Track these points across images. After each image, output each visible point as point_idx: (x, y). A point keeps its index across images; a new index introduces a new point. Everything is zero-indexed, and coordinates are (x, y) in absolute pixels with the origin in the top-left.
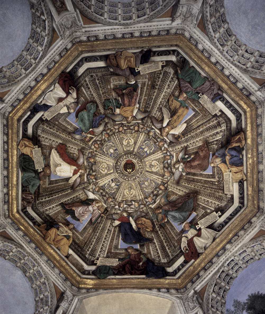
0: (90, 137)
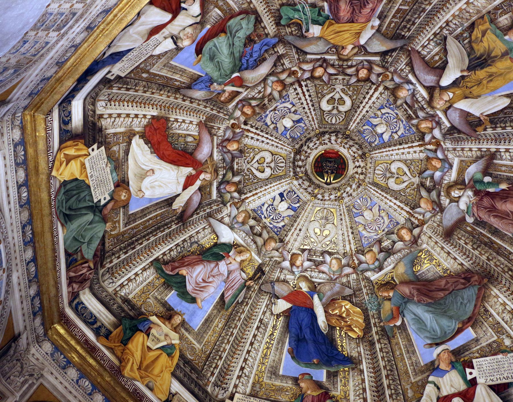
0: (233, 92)
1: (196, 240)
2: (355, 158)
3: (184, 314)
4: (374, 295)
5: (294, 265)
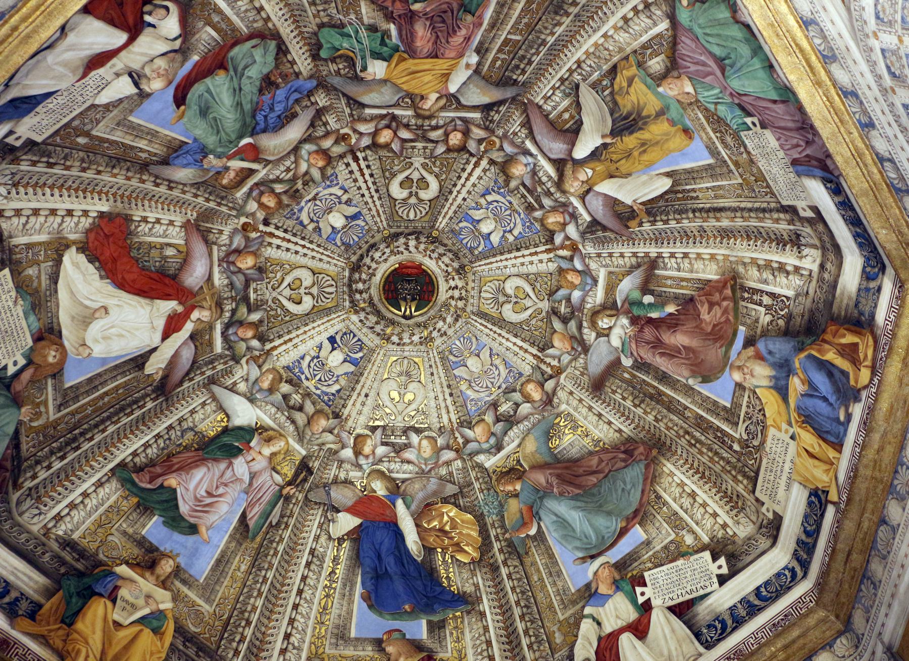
0: (242, 169)
1: (191, 425)
2: (449, 274)
3: (178, 555)
4: (492, 490)
5: (360, 453)
